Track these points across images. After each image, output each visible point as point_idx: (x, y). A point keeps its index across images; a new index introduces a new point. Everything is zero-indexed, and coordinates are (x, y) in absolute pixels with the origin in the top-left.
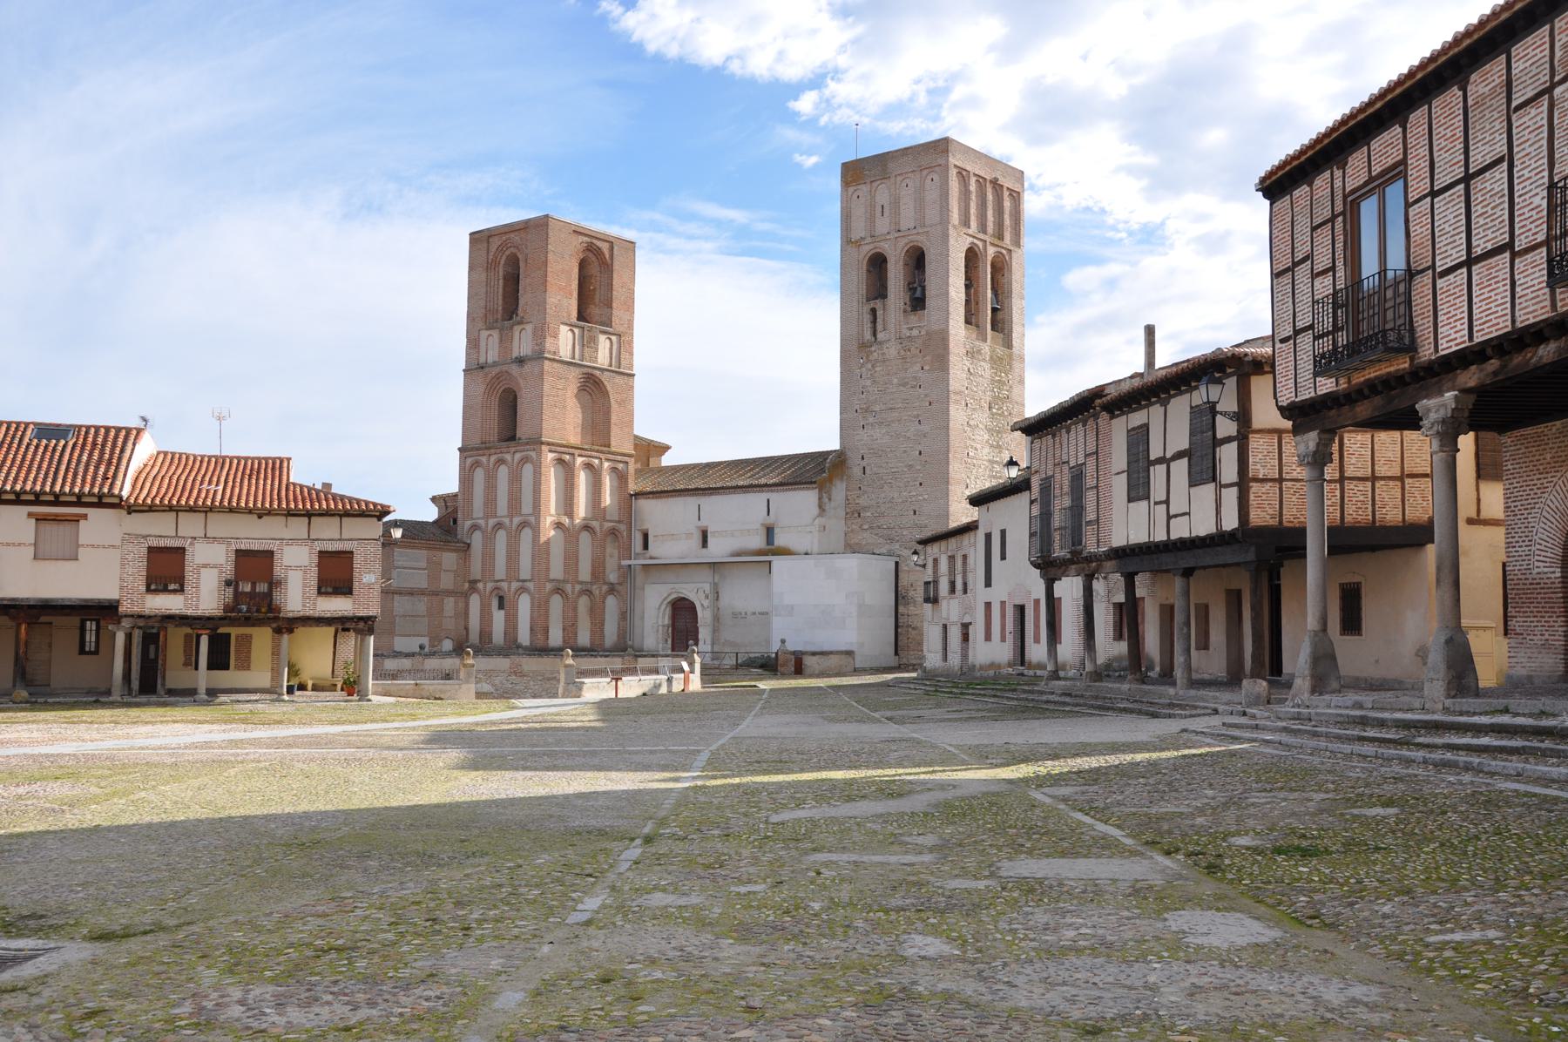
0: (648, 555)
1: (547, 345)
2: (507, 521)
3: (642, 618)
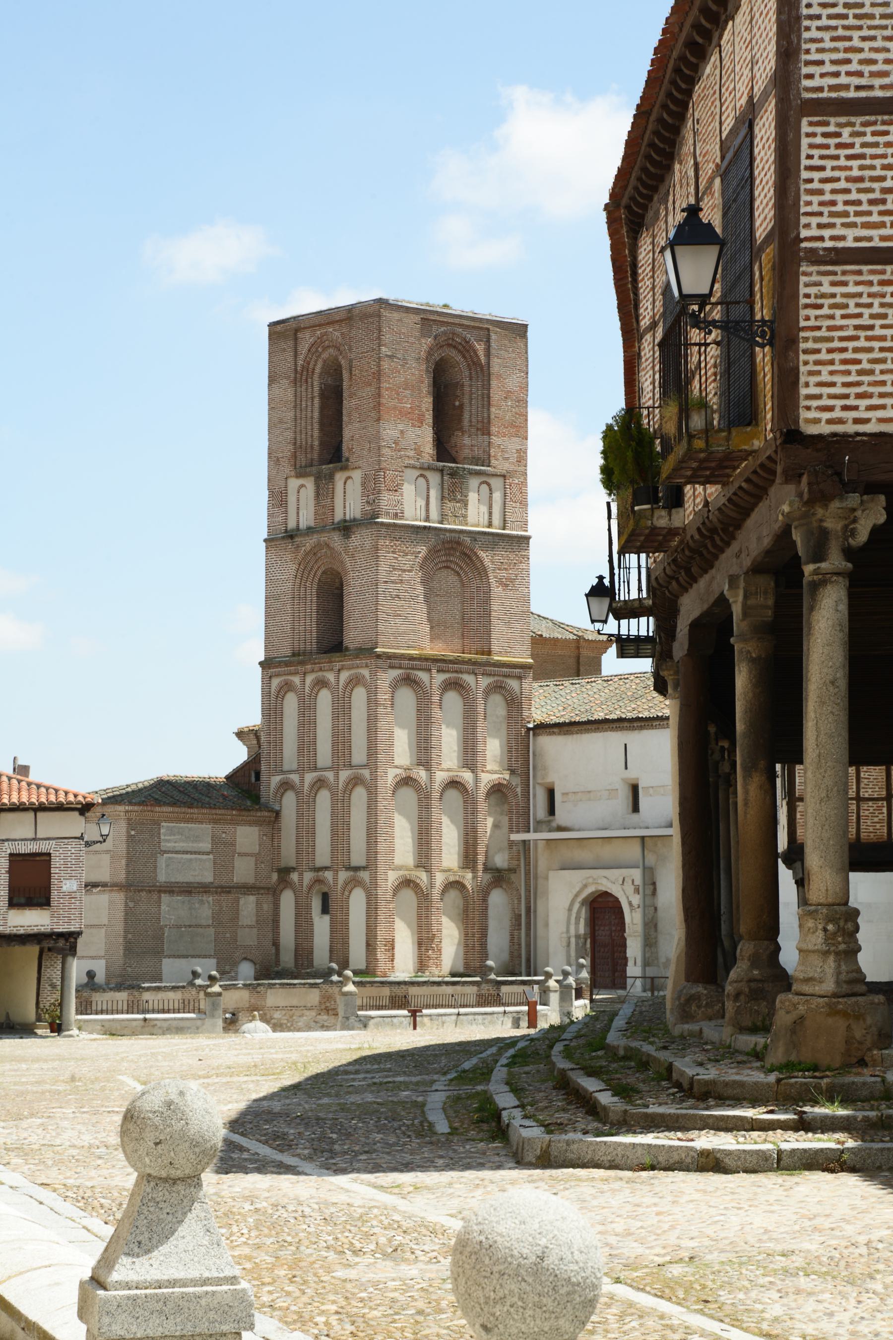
0: (554, 825)
1: (383, 503)
2: (330, 775)
3: (547, 925)
